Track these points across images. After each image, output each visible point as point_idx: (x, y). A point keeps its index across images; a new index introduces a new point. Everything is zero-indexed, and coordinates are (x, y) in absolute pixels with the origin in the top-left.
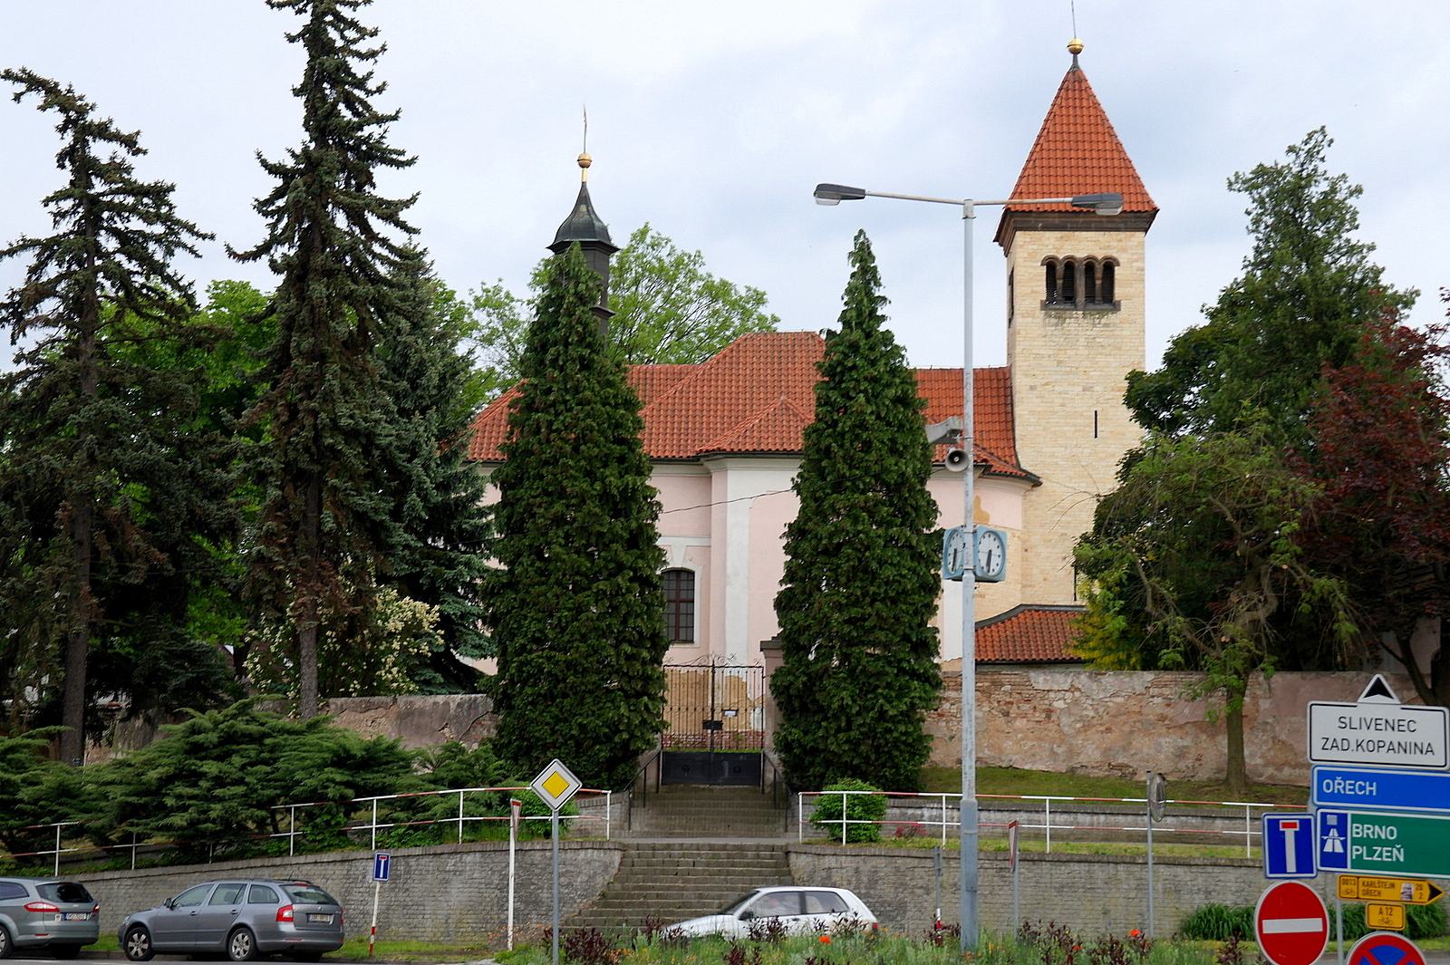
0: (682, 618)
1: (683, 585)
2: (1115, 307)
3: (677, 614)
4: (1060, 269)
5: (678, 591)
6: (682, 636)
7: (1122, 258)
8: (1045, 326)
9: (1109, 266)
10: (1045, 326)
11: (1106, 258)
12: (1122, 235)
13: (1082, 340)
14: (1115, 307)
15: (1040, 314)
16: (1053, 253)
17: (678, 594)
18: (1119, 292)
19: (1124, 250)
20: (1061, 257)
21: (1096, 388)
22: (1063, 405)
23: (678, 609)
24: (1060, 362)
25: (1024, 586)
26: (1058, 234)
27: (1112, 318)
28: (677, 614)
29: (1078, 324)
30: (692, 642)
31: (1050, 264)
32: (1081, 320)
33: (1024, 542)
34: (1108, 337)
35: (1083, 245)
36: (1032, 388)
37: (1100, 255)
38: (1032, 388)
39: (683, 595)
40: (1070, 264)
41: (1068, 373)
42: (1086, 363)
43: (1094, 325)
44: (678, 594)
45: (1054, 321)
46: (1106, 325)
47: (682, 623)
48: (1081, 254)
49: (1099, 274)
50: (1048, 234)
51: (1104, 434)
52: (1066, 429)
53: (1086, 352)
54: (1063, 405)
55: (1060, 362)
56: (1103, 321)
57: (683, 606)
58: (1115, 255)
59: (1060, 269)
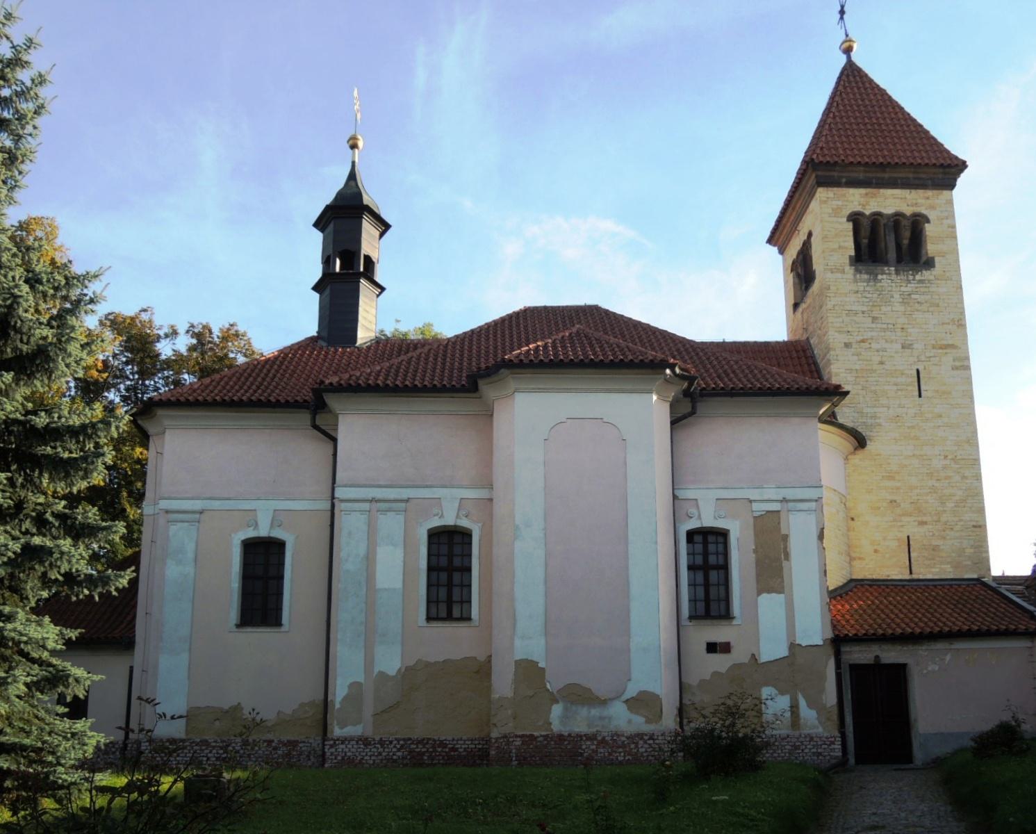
0: (456, 591)
1: (457, 550)
2: (930, 264)
5: (450, 557)
6: (456, 612)
7: (931, 215)
9: (917, 223)
10: (856, 281)
12: (929, 193)
13: (897, 296)
14: (930, 264)
15: (850, 271)
16: (859, 209)
17: (450, 561)
18: (931, 248)
19: (932, 207)
20: (867, 213)
21: (915, 346)
22: (882, 363)
23: (450, 578)
24: (874, 319)
26: (862, 191)
27: (926, 274)
28: (450, 585)
29: (891, 281)
30: (469, 619)
31: (855, 218)
32: (894, 277)
34: (924, 293)
35: (891, 202)
36: (847, 345)
37: (908, 211)
38: (847, 345)
39: (457, 562)
41: (884, 330)
42: (902, 320)
43: (909, 281)
44: (450, 561)
45: (866, 277)
46: (921, 281)
47: (456, 597)
48: (889, 210)
49: (906, 234)
50: (852, 191)
51: (929, 394)
52: (886, 387)
53: (902, 308)
54: (882, 363)
55: (874, 319)
56: (918, 277)
58: (924, 211)
59: (866, 223)
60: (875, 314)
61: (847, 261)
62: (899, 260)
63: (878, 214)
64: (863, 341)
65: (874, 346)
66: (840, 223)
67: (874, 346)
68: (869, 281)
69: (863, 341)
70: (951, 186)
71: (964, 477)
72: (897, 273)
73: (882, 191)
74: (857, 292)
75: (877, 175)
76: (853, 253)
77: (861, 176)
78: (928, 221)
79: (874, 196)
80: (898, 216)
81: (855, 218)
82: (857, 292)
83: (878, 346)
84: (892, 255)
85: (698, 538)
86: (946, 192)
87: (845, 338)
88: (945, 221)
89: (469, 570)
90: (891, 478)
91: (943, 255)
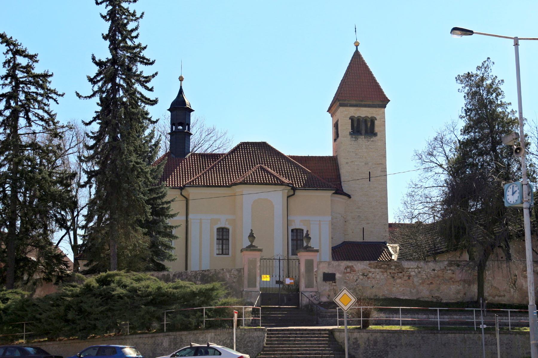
7: (378, 117)
9: (373, 121)
11: (372, 117)
15: (349, 137)
16: (353, 115)
18: (377, 129)
24: (356, 154)
27: (374, 138)
29: (362, 140)
35: (364, 112)
37: (370, 116)
38: (347, 163)
43: (368, 141)
45: (354, 139)
46: (372, 141)
49: (369, 124)
54: (358, 169)
55: (356, 154)
56: (371, 139)
58: (375, 116)
61: (348, 134)
64: (352, 162)
67: (356, 163)
68: (355, 141)
70: (385, 107)
71: (382, 208)
76: (351, 131)
78: (376, 120)
84: (363, 132)
85: (295, 231)
86: (383, 109)
90: (359, 208)
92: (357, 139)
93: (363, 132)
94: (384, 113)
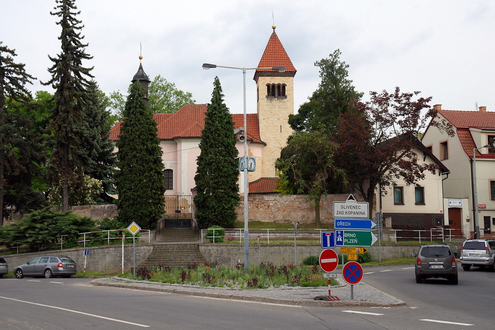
1: (170, 174)
3: (168, 181)
4: (271, 87)
5: (168, 175)
6: (170, 188)
8: (267, 102)
9: (284, 86)
10: (267, 102)
11: (283, 84)
12: (287, 78)
13: (277, 106)
14: (286, 97)
18: (286, 93)
19: (288, 82)
21: (281, 119)
22: (272, 124)
23: (168, 180)
24: (271, 112)
25: (262, 173)
27: (285, 100)
28: (168, 181)
29: (276, 102)
30: (173, 189)
31: (268, 86)
33: (262, 161)
34: (284, 105)
35: (277, 80)
39: (170, 177)
40: (273, 85)
42: (278, 112)
43: (280, 102)
45: (269, 101)
46: (283, 102)
47: (170, 184)
48: (276, 83)
49: (281, 88)
50: (267, 77)
54: (272, 124)
55: (271, 112)
57: (170, 179)
58: (286, 83)
59: (271, 87)
60: (271, 111)
62: (279, 95)
63: (274, 84)
64: (268, 118)
65: (270, 119)
66: (264, 87)
67: (271, 119)
69: (268, 118)
72: (278, 100)
73: (275, 77)
74: (267, 105)
75: (274, 73)
77: (270, 74)
79: (273, 79)
80: (279, 86)
81: (268, 86)
82: (267, 105)
83: (272, 119)
84: (276, 95)
87: (264, 117)
88: (291, 86)
89: (172, 178)
91: (289, 95)
92: (271, 100)
93: (276, 95)
94: (292, 80)
